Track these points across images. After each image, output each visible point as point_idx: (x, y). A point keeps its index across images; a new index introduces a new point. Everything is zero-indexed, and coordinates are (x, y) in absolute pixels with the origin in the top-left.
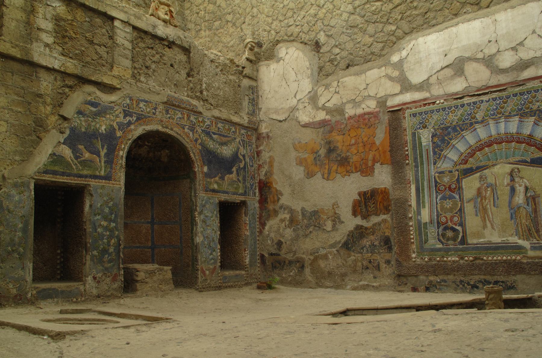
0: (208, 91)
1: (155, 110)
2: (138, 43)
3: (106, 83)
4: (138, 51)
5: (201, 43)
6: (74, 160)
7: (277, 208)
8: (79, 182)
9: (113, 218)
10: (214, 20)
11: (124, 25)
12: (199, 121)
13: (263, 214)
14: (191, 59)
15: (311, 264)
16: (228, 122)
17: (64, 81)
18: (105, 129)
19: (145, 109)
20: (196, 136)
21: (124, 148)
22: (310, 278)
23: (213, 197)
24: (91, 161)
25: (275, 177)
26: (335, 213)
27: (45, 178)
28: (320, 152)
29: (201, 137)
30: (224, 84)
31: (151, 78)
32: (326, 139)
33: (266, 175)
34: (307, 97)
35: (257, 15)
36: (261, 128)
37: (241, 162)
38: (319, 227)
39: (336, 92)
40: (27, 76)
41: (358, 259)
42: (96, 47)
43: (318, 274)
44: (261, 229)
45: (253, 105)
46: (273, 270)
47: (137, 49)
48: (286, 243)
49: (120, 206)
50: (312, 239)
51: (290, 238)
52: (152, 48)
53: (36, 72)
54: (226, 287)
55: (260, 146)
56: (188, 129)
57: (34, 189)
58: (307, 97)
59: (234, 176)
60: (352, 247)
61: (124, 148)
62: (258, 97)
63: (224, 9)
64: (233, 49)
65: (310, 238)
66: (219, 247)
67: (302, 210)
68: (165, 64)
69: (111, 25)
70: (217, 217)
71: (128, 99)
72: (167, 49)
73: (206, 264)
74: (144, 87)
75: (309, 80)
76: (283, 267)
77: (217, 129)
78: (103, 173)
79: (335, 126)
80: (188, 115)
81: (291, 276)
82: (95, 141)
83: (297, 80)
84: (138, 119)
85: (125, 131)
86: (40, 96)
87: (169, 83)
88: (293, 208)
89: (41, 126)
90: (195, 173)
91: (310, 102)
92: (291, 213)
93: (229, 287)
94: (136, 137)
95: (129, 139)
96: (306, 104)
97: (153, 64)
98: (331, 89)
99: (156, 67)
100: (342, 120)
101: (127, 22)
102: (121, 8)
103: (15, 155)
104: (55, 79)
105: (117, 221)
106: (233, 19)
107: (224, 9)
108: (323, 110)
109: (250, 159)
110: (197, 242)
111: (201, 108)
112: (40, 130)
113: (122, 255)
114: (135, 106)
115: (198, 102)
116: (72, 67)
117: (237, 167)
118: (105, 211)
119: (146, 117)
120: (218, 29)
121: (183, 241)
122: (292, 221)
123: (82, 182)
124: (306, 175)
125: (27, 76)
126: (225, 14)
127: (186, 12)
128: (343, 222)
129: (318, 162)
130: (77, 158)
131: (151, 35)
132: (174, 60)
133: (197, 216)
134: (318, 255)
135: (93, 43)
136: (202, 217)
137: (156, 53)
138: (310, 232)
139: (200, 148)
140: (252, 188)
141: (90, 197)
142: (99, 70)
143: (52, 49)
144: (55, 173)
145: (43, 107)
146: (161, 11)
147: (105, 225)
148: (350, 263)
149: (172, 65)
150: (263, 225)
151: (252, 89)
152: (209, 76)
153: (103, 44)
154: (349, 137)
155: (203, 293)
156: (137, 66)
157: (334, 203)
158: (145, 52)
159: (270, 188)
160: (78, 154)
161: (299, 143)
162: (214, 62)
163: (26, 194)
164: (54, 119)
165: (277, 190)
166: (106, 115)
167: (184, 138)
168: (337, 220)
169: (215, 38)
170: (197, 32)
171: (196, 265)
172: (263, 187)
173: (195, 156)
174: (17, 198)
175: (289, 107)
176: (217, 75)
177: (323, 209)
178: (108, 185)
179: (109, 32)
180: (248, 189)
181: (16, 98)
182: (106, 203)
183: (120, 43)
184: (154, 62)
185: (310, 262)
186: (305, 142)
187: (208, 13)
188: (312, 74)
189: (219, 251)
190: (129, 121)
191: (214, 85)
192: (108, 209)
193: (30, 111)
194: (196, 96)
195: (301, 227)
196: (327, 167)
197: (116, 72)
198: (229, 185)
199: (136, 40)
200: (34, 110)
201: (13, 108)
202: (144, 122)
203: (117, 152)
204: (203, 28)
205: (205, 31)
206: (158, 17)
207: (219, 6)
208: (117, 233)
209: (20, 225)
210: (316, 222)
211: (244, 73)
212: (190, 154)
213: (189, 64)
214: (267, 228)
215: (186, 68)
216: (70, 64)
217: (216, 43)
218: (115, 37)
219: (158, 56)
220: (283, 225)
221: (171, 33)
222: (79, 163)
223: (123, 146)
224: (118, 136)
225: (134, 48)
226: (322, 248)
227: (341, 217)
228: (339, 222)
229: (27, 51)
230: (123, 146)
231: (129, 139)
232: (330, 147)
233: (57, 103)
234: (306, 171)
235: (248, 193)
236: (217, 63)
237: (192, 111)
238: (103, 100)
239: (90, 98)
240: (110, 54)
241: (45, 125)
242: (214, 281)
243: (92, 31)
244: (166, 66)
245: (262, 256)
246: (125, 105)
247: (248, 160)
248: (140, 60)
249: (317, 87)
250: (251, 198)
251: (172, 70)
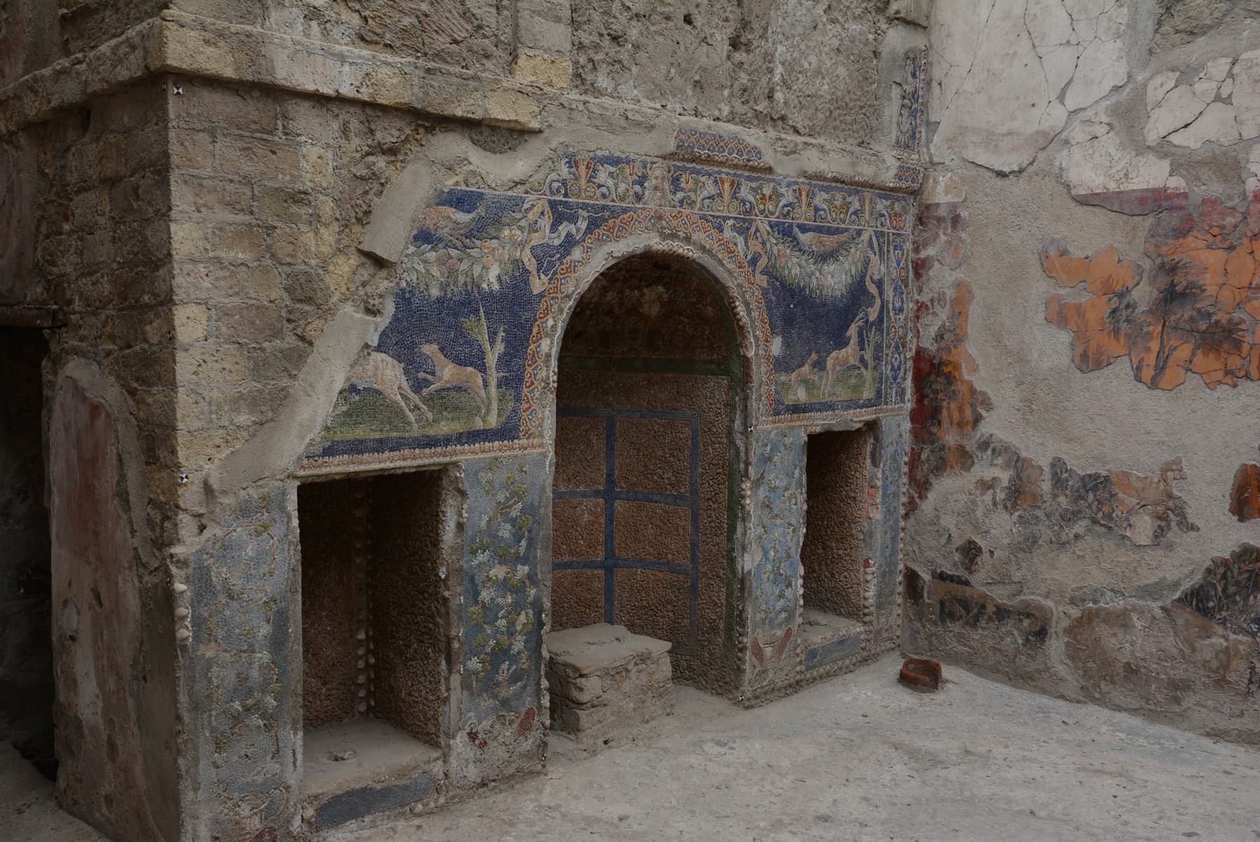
0: (789, 88)
1: (641, 184)
3: (498, 120)
6: (412, 395)
7: (970, 446)
8: (426, 461)
9: (522, 550)
12: (764, 195)
13: (924, 456)
15: (1069, 631)
16: (843, 182)
17: (372, 132)
18: (499, 278)
19: (613, 189)
20: (755, 246)
21: (554, 327)
22: (1061, 670)
23: (792, 428)
24: (458, 389)
25: (971, 348)
26: (1170, 496)
27: (328, 470)
28: (1135, 295)
29: (768, 246)
30: (832, 54)
31: (627, 74)
32: (1159, 255)
33: (942, 337)
34: (1104, 104)
36: (934, 188)
37: (871, 305)
38: (1107, 523)
39: (1218, 98)
40: (259, 135)
41: (1237, 651)
43: (1091, 664)
44: (912, 498)
45: (913, 114)
46: (943, 621)
48: (991, 552)
49: (542, 511)
50: (1079, 557)
51: (1006, 541)
53: (285, 117)
54: (815, 679)
55: (925, 245)
56: (734, 228)
57: (299, 510)
58: (1104, 104)
59: (849, 353)
60: (1220, 610)
61: (554, 327)
62: (929, 83)
65: (1073, 553)
66: (802, 572)
67: (1053, 466)
68: (668, 18)
70: (801, 485)
71: (563, 161)
73: (767, 627)
74: (609, 114)
75: (1119, 44)
76: (976, 619)
77: (812, 213)
78: (493, 421)
79: (1201, 215)
80: (732, 184)
81: (999, 650)
82: (468, 323)
83: (1074, 41)
84: (594, 224)
85: (555, 273)
86: (299, 197)
87: (679, 81)
88: (1023, 454)
89: (309, 300)
90: (746, 362)
91: (1116, 123)
92: (1016, 467)
93: (821, 677)
94: (587, 286)
95: (568, 297)
96: (1098, 127)
97: (634, 23)
98: (1200, 87)
99: (641, 34)
100: (1230, 197)
103: (237, 411)
104: (345, 131)
105: (535, 557)
108: (1165, 155)
109: (895, 289)
110: (746, 570)
111: (771, 153)
112: (305, 314)
113: (545, 654)
114: (583, 181)
115: (761, 133)
116: (395, 81)
117: (860, 323)
118: (500, 534)
119: (614, 214)
121: (701, 556)
122: (1017, 491)
123: (436, 460)
124: (1077, 361)
125: (259, 135)
128: (1193, 528)
129: (1124, 326)
130: (418, 386)
133: (749, 493)
134: (1098, 611)
136: (762, 493)
138: (1077, 537)
139: (765, 284)
140: (895, 378)
141: (459, 499)
142: (475, 78)
143: (328, 25)
144: (357, 447)
145: (311, 235)
147: (501, 576)
148: (1207, 654)
149: (688, 20)
150: (921, 486)
151: (914, 60)
152: (794, 36)
154: (1249, 260)
155: (756, 711)
156: (586, 39)
157: (1167, 464)
159: (950, 379)
160: (421, 375)
161: (1061, 256)
163: (278, 530)
164: (346, 269)
165: (973, 391)
166: (500, 230)
167: (720, 262)
168: (1172, 516)
171: (741, 635)
172: (929, 374)
173: (749, 311)
174: (250, 551)
175: (1037, 132)
176: (815, 27)
177: (1126, 475)
178: (507, 453)
180: (886, 381)
181: (229, 217)
182: (503, 508)
184: (637, 15)
185: (1066, 623)
186: (1081, 255)
188: (1132, 25)
189: (800, 581)
190: (569, 235)
191: (806, 65)
192: (508, 526)
193: (273, 256)
194: (757, 114)
195: (1048, 516)
196: (1155, 345)
197: (524, 75)
198: (838, 380)
200: (284, 250)
201: (222, 254)
202: (611, 230)
203: (532, 346)
208: (533, 591)
209: (265, 630)
210: (1099, 510)
212: (736, 307)
214: (931, 496)
215: (727, 20)
216: (386, 70)
220: (988, 497)
222: (425, 401)
223: (551, 322)
224: (535, 292)
226: (1112, 590)
227: (1189, 511)
228: (1179, 524)
229: (251, 47)
230: (551, 322)
231: (568, 297)
232: (1173, 285)
233: (353, 215)
234: (1080, 349)
235: (886, 394)
237: (745, 167)
238: (490, 180)
239: (451, 182)
240: (506, 12)
241: (320, 295)
242: (786, 672)
244: (671, 24)
245: (911, 578)
246: (556, 185)
247: (889, 292)
248: (596, 16)
249: (1147, 74)
250: (892, 410)
251: (687, 36)
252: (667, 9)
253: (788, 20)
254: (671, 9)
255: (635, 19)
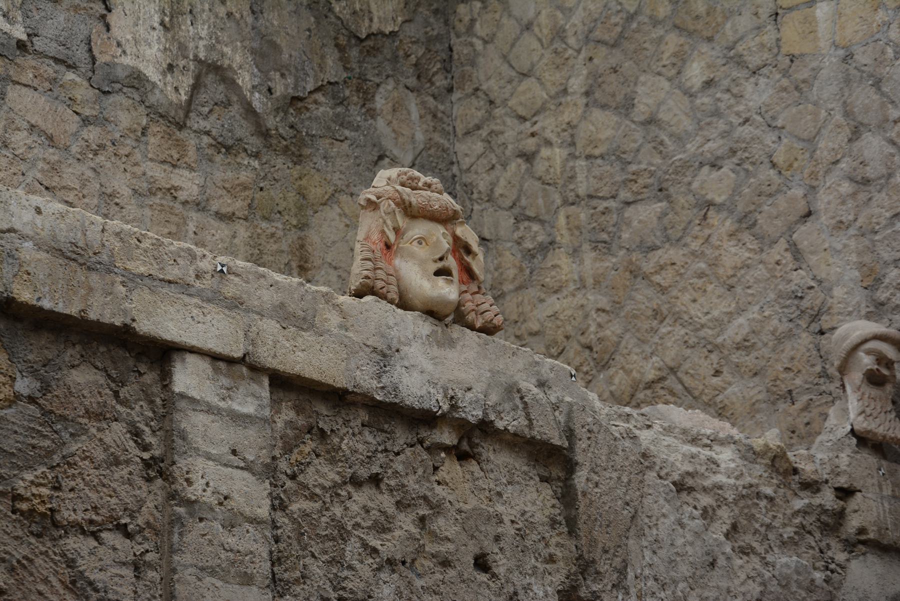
2: (303, 466)
4: (305, 514)
5: (554, 316)
10: (624, 195)
11: (225, 381)
14: (582, 503)
35: (890, 176)
42: (75, 543)
47: (297, 506)
52: (375, 480)
63: (680, 139)
64: (749, 360)
68: (446, 563)
69: (156, 389)
72: (451, 469)
97: (384, 576)
101: (242, 361)
102: (208, 283)
106: (736, 191)
107: (680, 139)
120: (654, 248)
126: (685, 165)
127: (461, 147)
131: (365, 406)
132: (492, 529)
135: (56, 525)
137: (398, 504)
146: (412, 256)
149: (482, 563)
152: (675, 582)
153: (112, 519)
158: (338, 511)
162: (691, 490)
169: (639, 297)
170: (530, 255)
176: (713, 564)
179: (149, 439)
183: (209, 498)
184: (390, 562)
187: (588, 157)
199: (288, 449)
204: (564, 237)
205: (575, 252)
206: (401, 295)
207: (651, 121)
211: (853, 523)
213: (572, 532)
215: (551, 559)
217: (645, 325)
218: (182, 463)
219: (406, 523)
221: (467, 376)
225: (279, 505)
236: (705, 490)
240: (151, 574)
243: (50, 453)
244: (452, 573)
248: (316, 569)
252: (444, 548)
253: (662, 553)
254: (451, 547)
255: (387, 569)
